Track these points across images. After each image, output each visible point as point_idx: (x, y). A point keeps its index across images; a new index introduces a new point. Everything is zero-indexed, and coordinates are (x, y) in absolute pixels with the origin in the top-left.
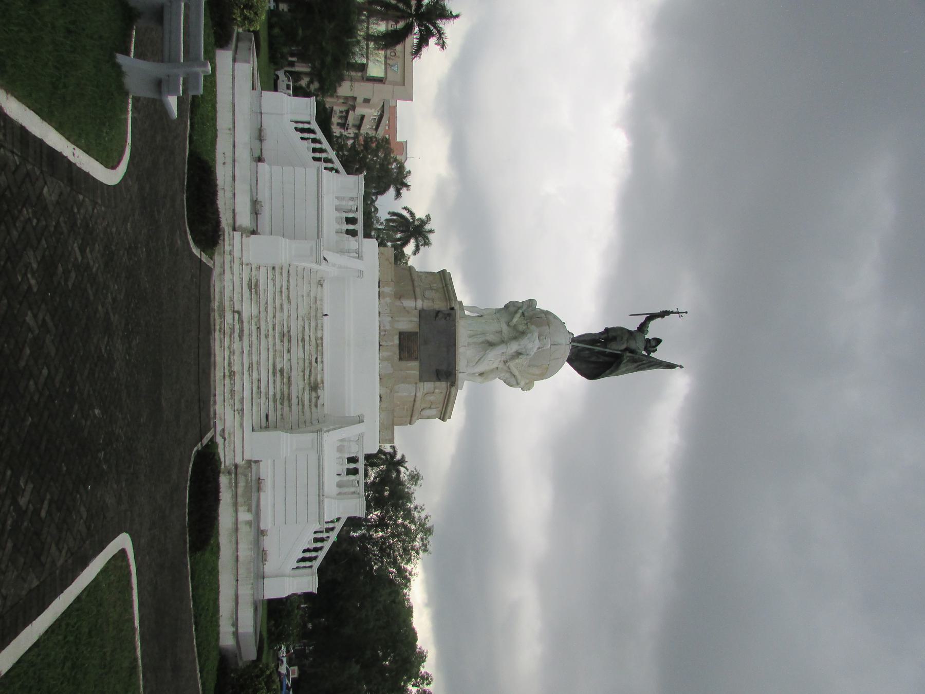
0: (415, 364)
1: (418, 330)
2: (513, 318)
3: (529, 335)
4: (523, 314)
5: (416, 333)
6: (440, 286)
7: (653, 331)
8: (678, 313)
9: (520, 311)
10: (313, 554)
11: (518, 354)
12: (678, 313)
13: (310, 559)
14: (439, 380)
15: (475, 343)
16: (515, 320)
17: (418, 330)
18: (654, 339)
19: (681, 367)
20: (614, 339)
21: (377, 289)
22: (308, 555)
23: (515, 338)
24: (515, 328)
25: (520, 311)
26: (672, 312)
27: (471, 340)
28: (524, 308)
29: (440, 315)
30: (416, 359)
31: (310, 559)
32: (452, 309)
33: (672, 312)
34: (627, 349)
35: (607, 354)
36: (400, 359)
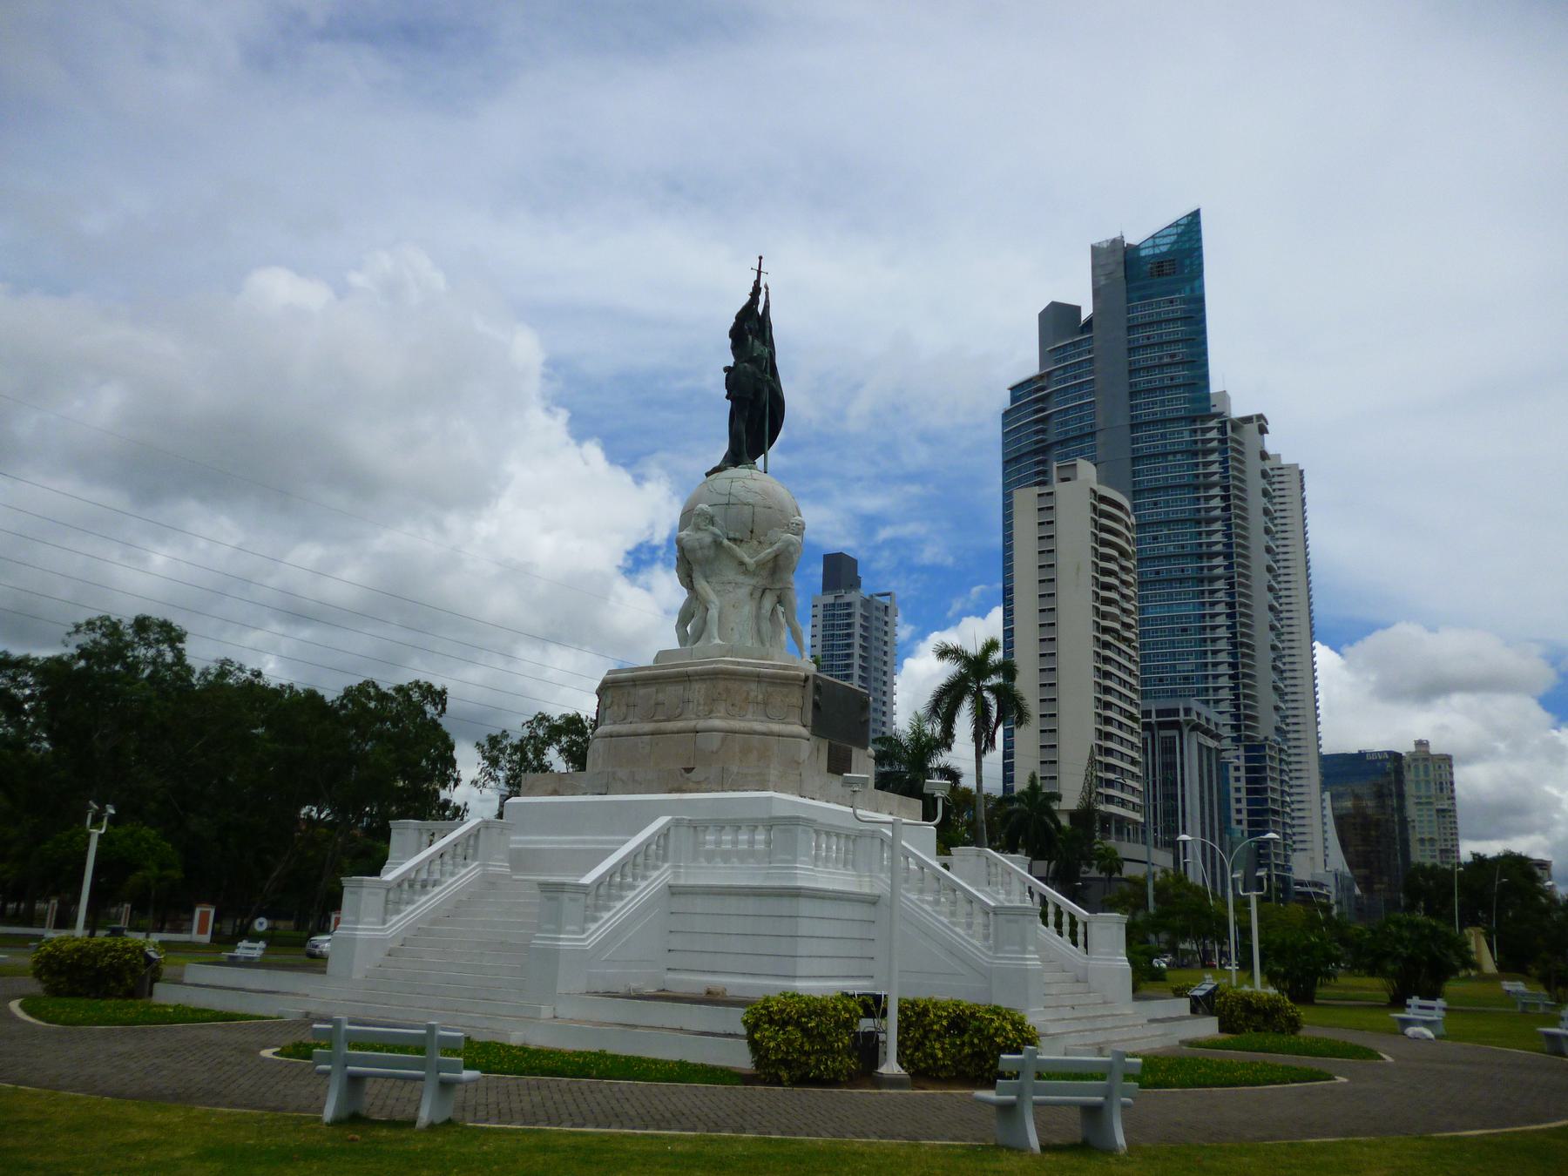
4: (734, 540)
6: (754, 686)
9: (726, 542)
10: (1066, 919)
13: (1073, 923)
16: (747, 559)
22: (1066, 928)
25: (726, 542)
28: (717, 531)
31: (1073, 923)
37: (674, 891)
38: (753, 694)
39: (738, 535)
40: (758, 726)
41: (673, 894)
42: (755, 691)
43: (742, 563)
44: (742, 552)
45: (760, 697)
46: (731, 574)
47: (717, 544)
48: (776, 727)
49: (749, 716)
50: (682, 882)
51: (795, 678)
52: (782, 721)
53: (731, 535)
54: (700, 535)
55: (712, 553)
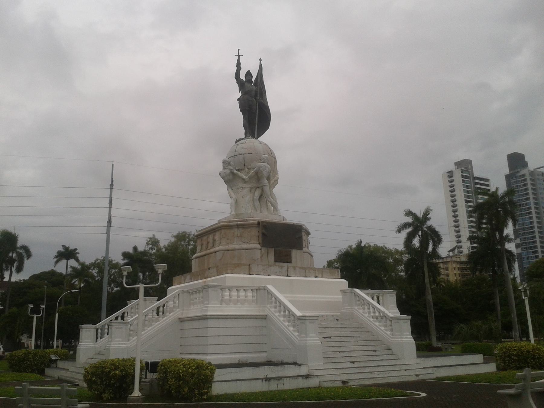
1: (273, 249)
3: (261, 169)
6: (236, 230)
8: (239, 56)
9: (235, 171)
11: (268, 179)
12: (239, 56)
14: (302, 237)
15: (261, 208)
16: (244, 177)
17: (273, 249)
21: (255, 276)
24: (250, 178)
25: (235, 171)
26: (238, 60)
27: (259, 211)
28: (231, 168)
32: (259, 223)
33: (238, 60)
34: (255, 99)
36: (291, 262)
37: (182, 320)
38: (236, 233)
39: (239, 168)
40: (237, 247)
41: (181, 321)
42: (236, 231)
43: (243, 179)
45: (239, 234)
46: (240, 185)
47: (232, 173)
48: (244, 246)
49: (235, 243)
50: (184, 316)
54: (226, 170)
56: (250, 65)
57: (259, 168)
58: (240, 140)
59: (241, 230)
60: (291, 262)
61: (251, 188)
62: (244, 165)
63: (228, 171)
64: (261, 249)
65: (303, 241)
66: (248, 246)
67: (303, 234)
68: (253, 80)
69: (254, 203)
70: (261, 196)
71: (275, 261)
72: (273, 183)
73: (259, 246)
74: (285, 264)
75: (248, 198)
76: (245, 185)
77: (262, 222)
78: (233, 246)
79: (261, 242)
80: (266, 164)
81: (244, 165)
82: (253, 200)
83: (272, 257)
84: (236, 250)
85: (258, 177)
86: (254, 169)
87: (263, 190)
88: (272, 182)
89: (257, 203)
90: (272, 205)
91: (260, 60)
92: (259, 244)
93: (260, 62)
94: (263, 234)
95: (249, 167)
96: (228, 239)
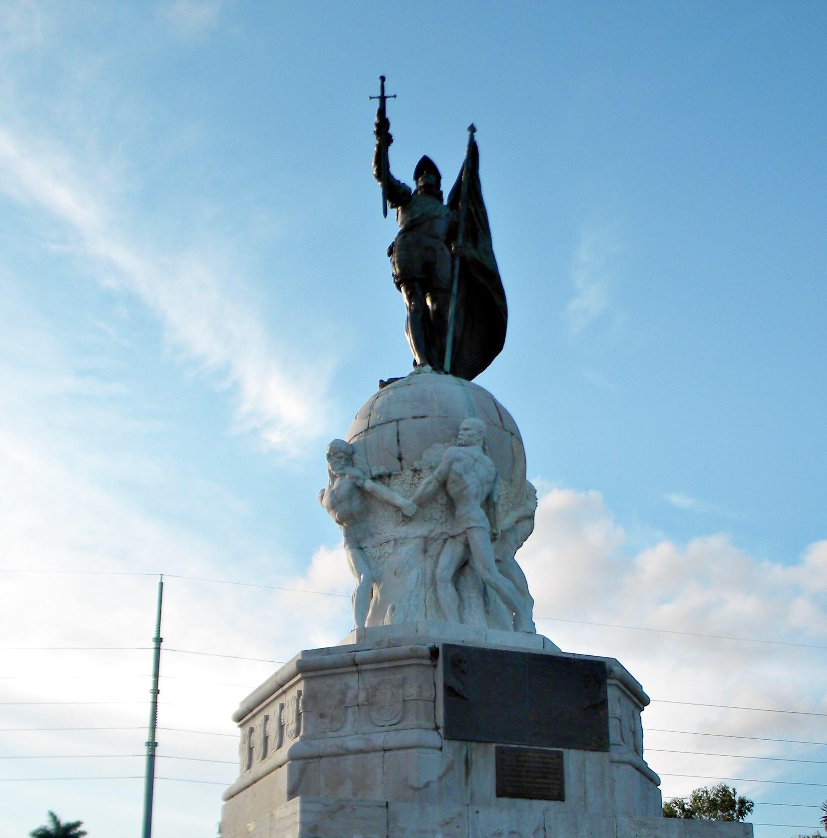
0: (572, 759)
1: (493, 746)
2: (388, 504)
3: (457, 467)
5: (500, 752)
6: (352, 680)
7: (404, 172)
9: (369, 484)
11: (489, 504)
14: (604, 703)
16: (400, 500)
18: (417, 175)
19: (472, 129)
20: (429, 267)
23: (451, 505)
24: (423, 503)
27: (453, 620)
28: (355, 472)
29: (457, 686)
30: (560, 756)
35: (455, 292)
36: (560, 797)
38: (351, 694)
39: (382, 470)
40: (353, 743)
43: (398, 509)
44: (398, 494)
45: (362, 697)
47: (359, 489)
48: (379, 739)
49: (348, 728)
51: (414, 655)
52: (395, 726)
53: (375, 472)
55: (356, 503)
56: (428, 140)
57: (451, 464)
58: (391, 380)
59: (370, 679)
60: (560, 797)
61: (427, 541)
62: (400, 459)
63: (344, 484)
64: (441, 749)
65: (612, 723)
66: (394, 739)
67: (612, 694)
68: (447, 186)
69: (435, 590)
70: (464, 565)
71: (501, 792)
72: (512, 529)
73: (434, 738)
74: (540, 805)
75: (413, 576)
76: (403, 530)
77: (447, 647)
78: (339, 741)
79: (441, 721)
80: (476, 450)
81: (400, 459)
82: (434, 582)
83: (485, 776)
84: (348, 752)
85: (446, 495)
86: (432, 468)
87: (467, 546)
88: (506, 521)
89: (447, 592)
90: (512, 607)
91: (472, 129)
92: (437, 728)
93: (472, 138)
94: (449, 690)
95: (416, 465)
96: (322, 716)
